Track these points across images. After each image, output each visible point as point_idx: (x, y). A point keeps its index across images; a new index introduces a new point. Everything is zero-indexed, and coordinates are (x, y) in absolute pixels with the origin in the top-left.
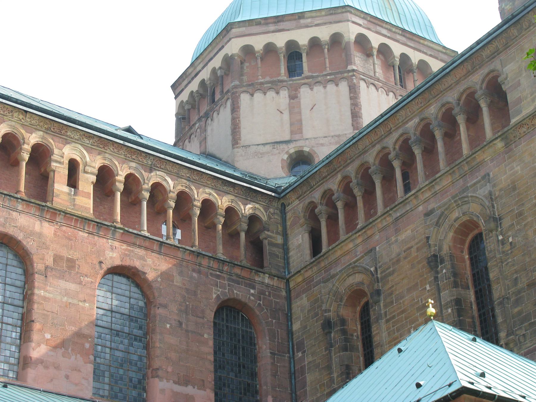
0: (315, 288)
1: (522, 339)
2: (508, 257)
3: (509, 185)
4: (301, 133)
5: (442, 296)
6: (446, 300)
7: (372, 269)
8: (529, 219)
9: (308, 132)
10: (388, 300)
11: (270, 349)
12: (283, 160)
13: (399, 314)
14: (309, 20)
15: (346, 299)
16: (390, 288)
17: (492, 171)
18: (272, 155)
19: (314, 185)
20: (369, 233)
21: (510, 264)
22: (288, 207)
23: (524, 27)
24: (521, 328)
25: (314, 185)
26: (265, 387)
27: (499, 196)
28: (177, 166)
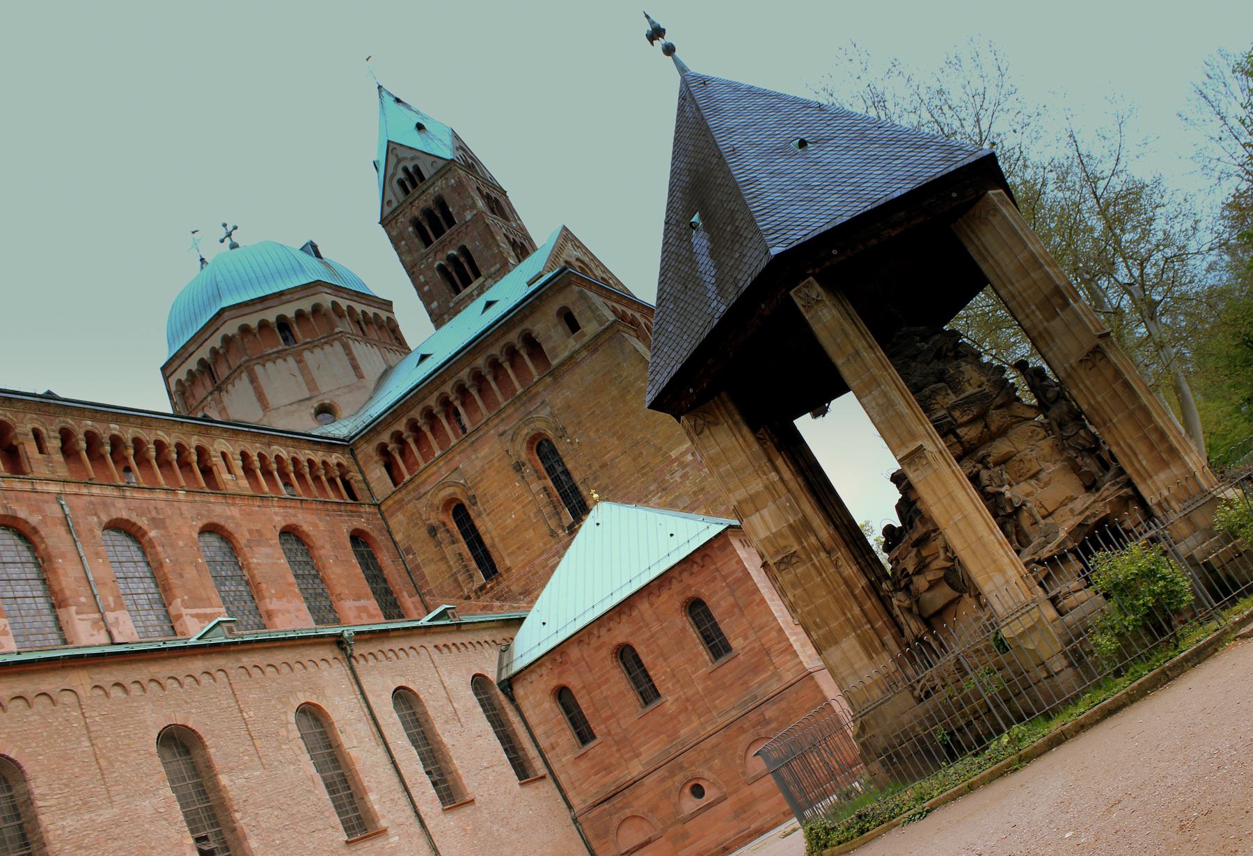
8: (588, 425)
9: (323, 389)
12: (311, 414)
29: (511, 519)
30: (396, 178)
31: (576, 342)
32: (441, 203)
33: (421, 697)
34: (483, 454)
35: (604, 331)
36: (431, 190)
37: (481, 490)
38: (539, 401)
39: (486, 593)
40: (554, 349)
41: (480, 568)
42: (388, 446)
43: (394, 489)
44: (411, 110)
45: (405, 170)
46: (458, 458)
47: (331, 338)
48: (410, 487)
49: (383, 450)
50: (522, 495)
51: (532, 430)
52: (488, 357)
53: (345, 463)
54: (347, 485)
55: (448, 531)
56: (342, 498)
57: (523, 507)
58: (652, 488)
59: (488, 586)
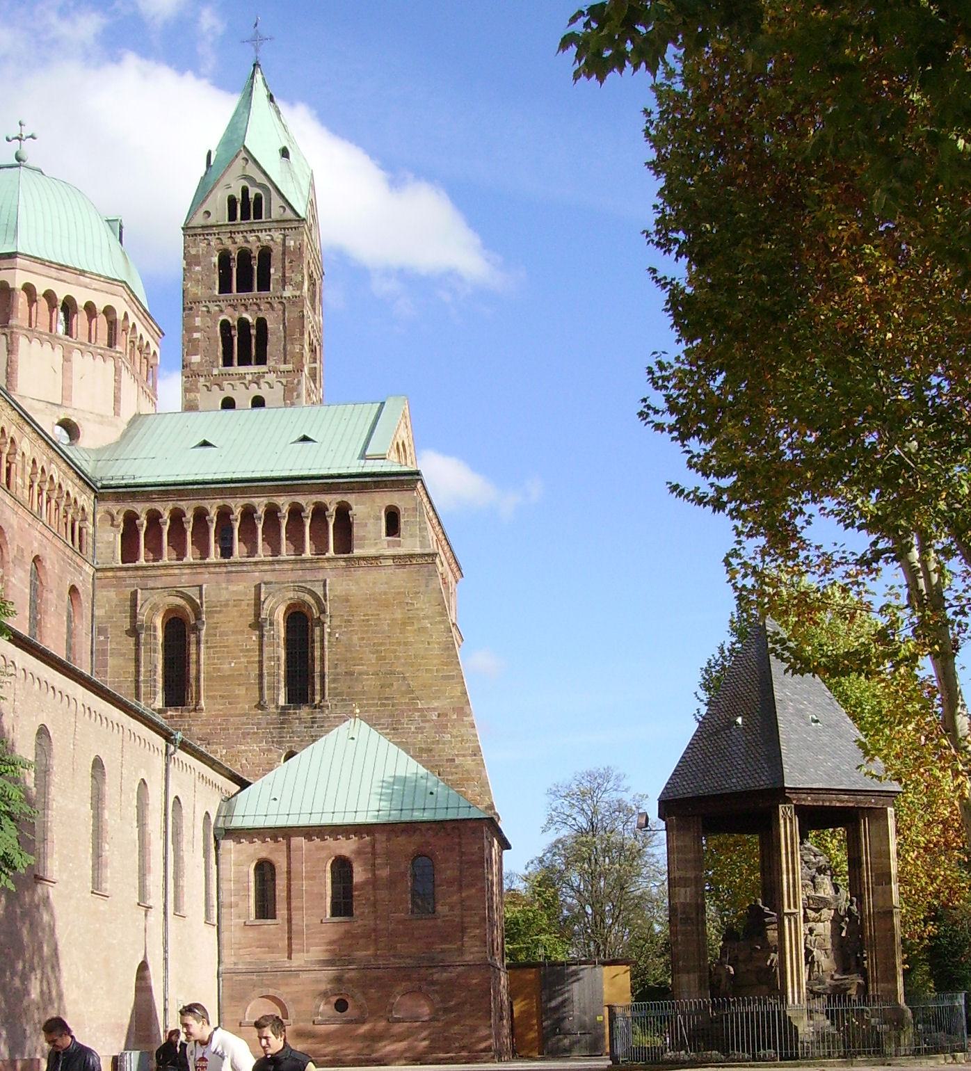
7: (198, 601)
9: (76, 403)
10: (211, 631)
13: (220, 647)
14: (88, 280)
29: (227, 667)
30: (230, 192)
32: (266, 254)
33: (183, 812)
34: (235, 589)
35: (422, 555)
36: (263, 235)
40: (363, 538)
42: (138, 519)
43: (120, 564)
44: (280, 120)
45: (245, 191)
47: (108, 353)
48: (140, 573)
49: (131, 518)
53: (86, 509)
54: (81, 529)
56: (73, 543)
57: (248, 662)
58: (382, 721)
59: (169, 713)
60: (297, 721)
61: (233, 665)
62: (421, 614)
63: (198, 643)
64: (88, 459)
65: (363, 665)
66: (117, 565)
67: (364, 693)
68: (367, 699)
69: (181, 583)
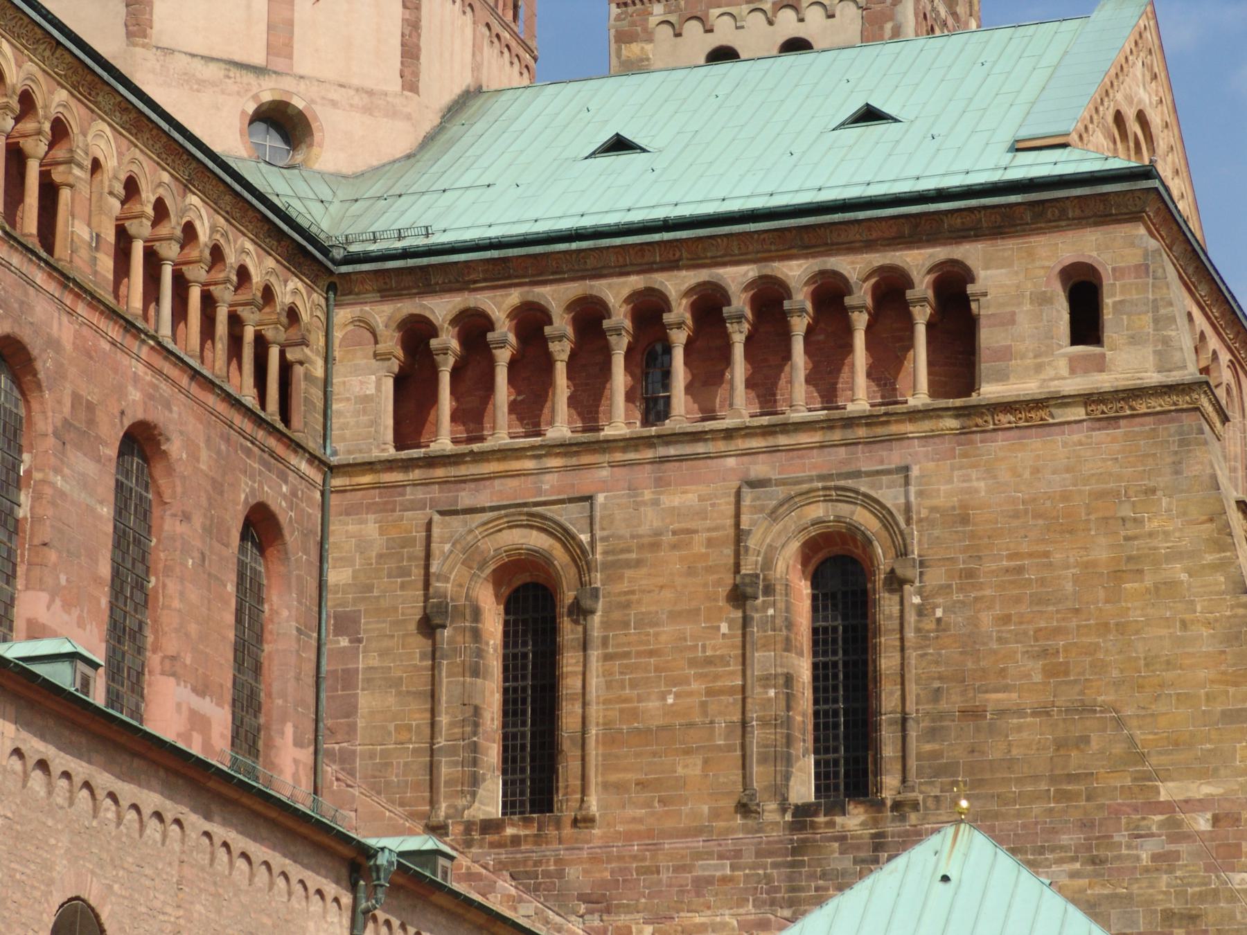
0: (405, 513)
1: (930, 803)
2: (928, 642)
3: (954, 508)
4: (290, 57)
5: (758, 660)
6: (766, 670)
7: (584, 538)
8: (988, 592)
10: (616, 615)
11: (297, 621)
13: (639, 654)
15: (494, 571)
16: (626, 593)
17: (920, 463)
18: (223, 92)
19: (437, 284)
20: (586, 459)
21: (929, 657)
22: (343, 298)
23: (1049, 214)
24: (932, 783)
25: (437, 284)
26: (280, 702)
27: (927, 518)
28: (222, 188)
31: (1073, 371)
37: (624, 586)
38: (894, 457)
39: (492, 845)
40: (1005, 354)
41: (504, 772)
42: (436, 335)
43: (391, 452)
46: (605, 473)
48: (440, 472)
50: (723, 661)
51: (838, 519)
52: (823, 273)
54: (286, 368)
55: (476, 635)
57: (710, 692)
58: (1065, 839)
59: (510, 831)
60: (836, 845)
61: (670, 701)
62: (1163, 546)
63: (585, 647)
64: (326, 193)
65: (1005, 689)
66: (384, 456)
67: (1010, 763)
68: (1019, 781)
69: (539, 492)
